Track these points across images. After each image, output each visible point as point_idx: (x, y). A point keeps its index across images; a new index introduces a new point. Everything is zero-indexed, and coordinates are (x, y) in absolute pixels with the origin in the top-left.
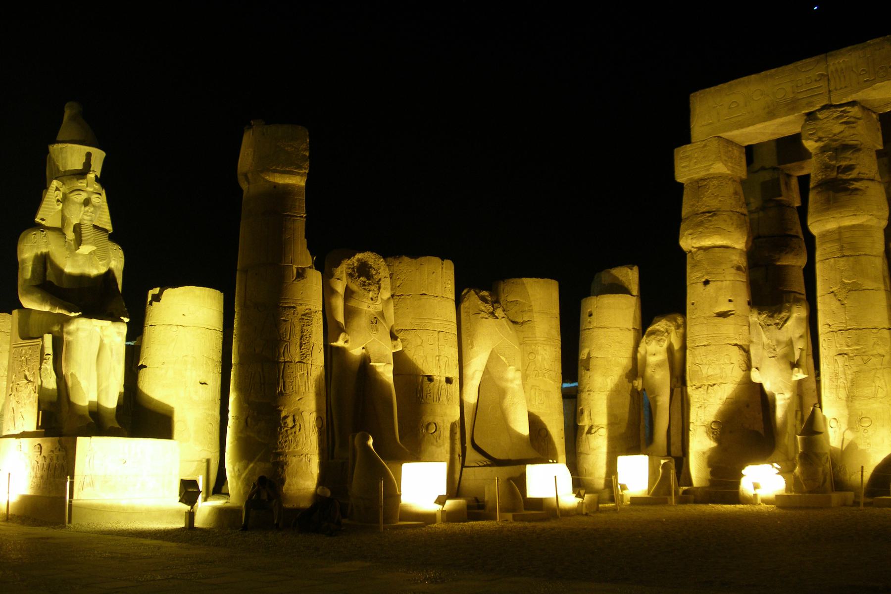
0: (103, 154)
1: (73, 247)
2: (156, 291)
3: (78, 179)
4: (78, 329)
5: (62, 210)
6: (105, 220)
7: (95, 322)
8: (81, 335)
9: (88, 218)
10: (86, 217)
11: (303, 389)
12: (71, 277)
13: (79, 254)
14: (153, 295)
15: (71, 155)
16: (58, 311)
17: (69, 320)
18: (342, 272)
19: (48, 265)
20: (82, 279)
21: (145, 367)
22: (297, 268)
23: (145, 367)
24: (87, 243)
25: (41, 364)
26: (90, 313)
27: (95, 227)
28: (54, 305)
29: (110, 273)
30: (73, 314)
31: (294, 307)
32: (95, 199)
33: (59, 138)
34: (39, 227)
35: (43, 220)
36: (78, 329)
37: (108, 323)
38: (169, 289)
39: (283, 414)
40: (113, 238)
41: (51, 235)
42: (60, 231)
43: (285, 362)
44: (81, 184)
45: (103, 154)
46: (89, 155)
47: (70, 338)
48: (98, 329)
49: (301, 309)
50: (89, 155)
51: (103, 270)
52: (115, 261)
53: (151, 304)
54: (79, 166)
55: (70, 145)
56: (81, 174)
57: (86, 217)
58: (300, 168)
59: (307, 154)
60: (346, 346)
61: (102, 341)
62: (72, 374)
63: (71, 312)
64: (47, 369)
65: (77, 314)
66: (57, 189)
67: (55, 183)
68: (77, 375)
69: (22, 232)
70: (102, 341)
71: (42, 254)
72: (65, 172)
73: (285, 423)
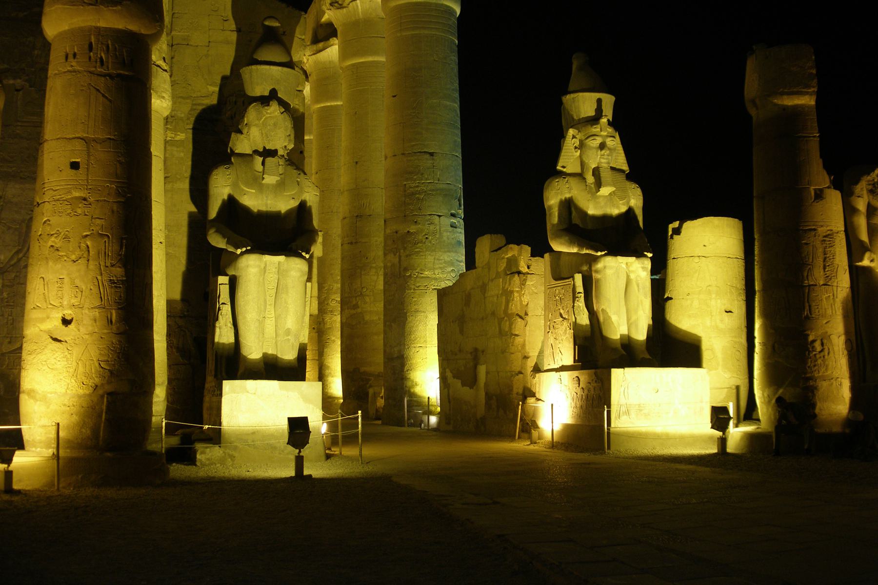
0: (613, 98)
1: (594, 190)
2: (676, 224)
3: (592, 126)
4: (605, 267)
5: (580, 156)
6: (621, 161)
7: (620, 259)
8: (609, 272)
10: (603, 161)
11: (829, 312)
12: (594, 218)
13: (600, 196)
14: (673, 229)
15: (584, 103)
16: (585, 251)
18: (862, 189)
19: (573, 209)
20: (605, 219)
21: (671, 299)
22: (815, 190)
23: (671, 299)
24: (606, 185)
25: (574, 302)
26: (615, 251)
27: (613, 169)
28: (581, 246)
29: (630, 211)
30: (599, 254)
31: (815, 230)
32: (610, 142)
33: (571, 88)
34: (561, 174)
35: (564, 167)
36: (605, 267)
37: (632, 260)
38: (688, 222)
39: (811, 338)
40: (630, 177)
41: (573, 181)
42: (580, 176)
43: (810, 286)
44: (595, 129)
45: (613, 98)
46: (599, 101)
47: (598, 276)
48: (624, 266)
49: (822, 231)
50: (599, 101)
51: (624, 209)
52: (634, 199)
53: (672, 237)
54: (592, 113)
55: (581, 94)
56: (594, 120)
57: (603, 161)
58: (808, 86)
59: (814, 71)
60: (872, 265)
61: (628, 276)
62: (603, 310)
64: (579, 307)
66: (574, 137)
67: (571, 132)
68: (608, 311)
69: (547, 180)
70: (628, 276)
71: (566, 199)
72: (579, 120)
73: (813, 347)
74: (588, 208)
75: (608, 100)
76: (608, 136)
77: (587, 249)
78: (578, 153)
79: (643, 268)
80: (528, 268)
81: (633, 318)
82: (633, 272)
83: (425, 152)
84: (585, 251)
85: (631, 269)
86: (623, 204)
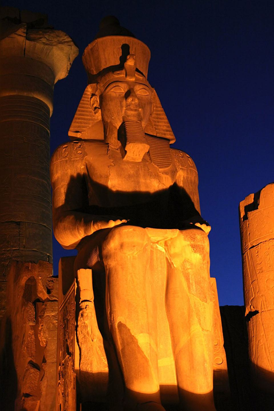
1: (120, 156)
2: (251, 199)
4: (122, 246)
9: (133, 113)
10: (130, 113)
13: (128, 162)
17: (104, 236)
21: (257, 312)
23: (257, 312)
24: (135, 140)
30: (112, 224)
36: (122, 246)
48: (161, 248)
51: (167, 183)
53: (246, 218)
62: (120, 325)
63: (107, 222)
65: (119, 222)
66: (93, 95)
67: (89, 90)
68: (129, 325)
70: (169, 265)
74: (107, 177)
75: (137, 45)
76: (136, 83)
77: (95, 222)
78: (98, 116)
79: (193, 246)
80: (49, 292)
81: (183, 340)
82: (176, 255)
83: (11, 222)
84: (93, 230)
85: (173, 251)
86: (166, 173)
